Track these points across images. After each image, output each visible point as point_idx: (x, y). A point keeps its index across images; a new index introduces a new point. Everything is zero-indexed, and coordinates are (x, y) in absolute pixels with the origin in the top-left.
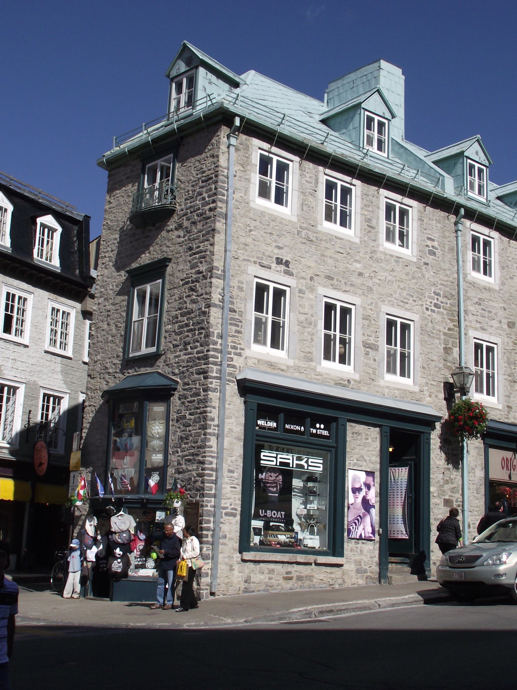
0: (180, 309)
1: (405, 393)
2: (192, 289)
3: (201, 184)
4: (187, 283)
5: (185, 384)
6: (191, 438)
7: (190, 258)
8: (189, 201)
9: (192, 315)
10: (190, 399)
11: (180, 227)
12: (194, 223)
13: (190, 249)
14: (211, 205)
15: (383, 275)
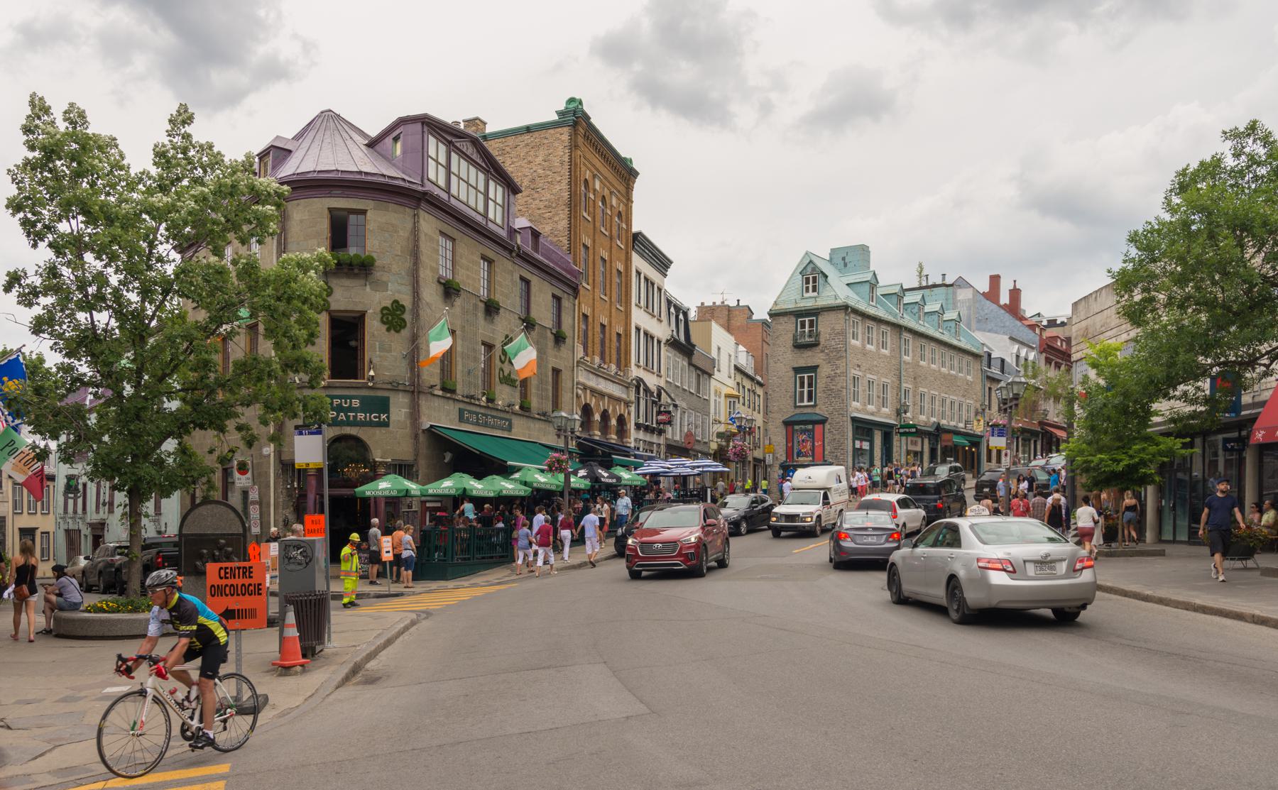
1: (887, 416)
11: (822, 351)
13: (829, 362)
15: (882, 365)
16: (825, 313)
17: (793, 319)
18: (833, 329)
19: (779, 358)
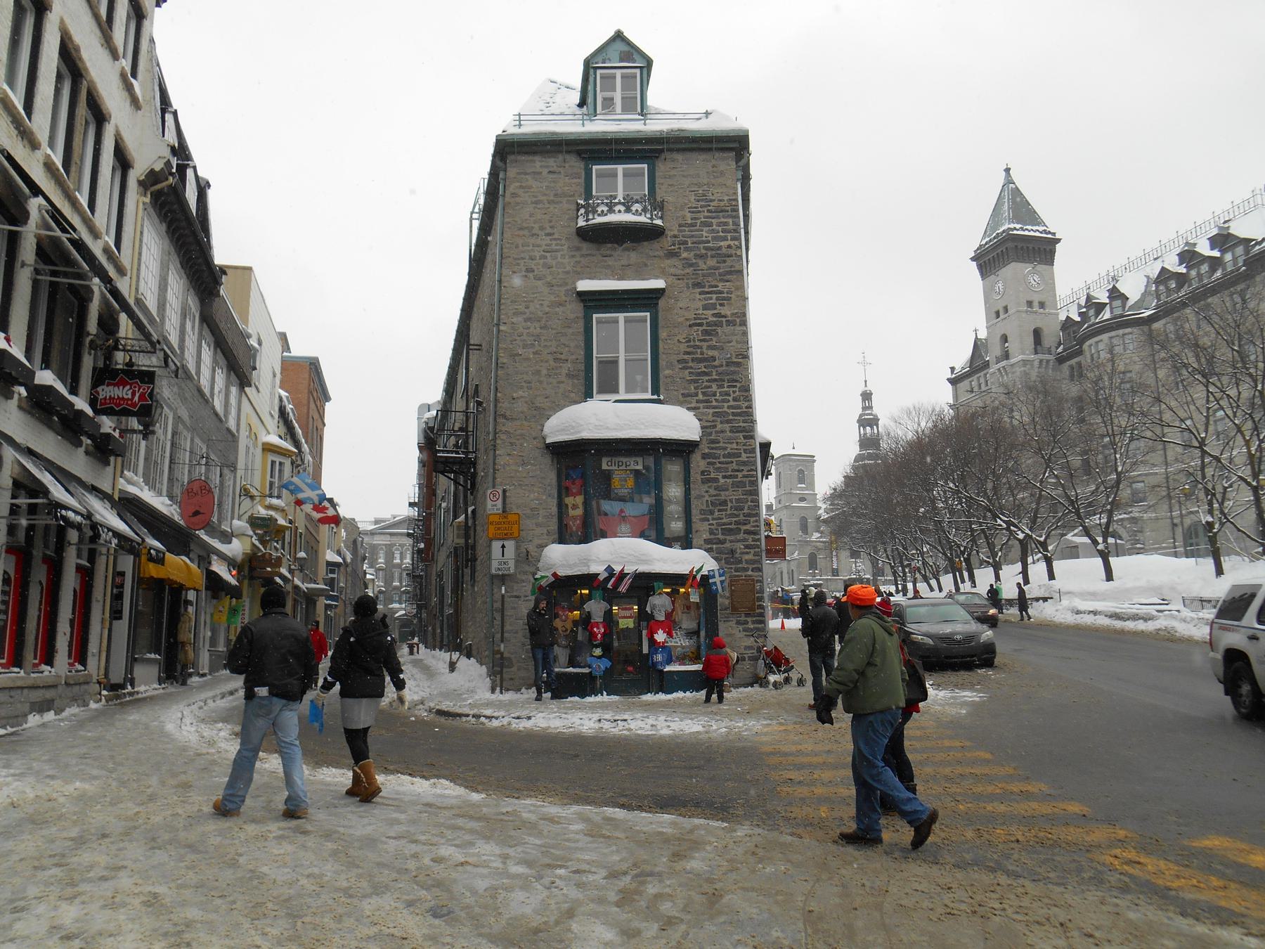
0: (688, 353)
2: (706, 332)
3: (706, 214)
4: (700, 325)
5: (713, 442)
6: (730, 505)
7: (698, 296)
8: (687, 229)
9: (716, 363)
10: (722, 460)
11: (672, 254)
12: (701, 256)
14: (732, 243)
16: (679, 157)
17: (575, 164)
18: (703, 198)
19: (532, 264)
